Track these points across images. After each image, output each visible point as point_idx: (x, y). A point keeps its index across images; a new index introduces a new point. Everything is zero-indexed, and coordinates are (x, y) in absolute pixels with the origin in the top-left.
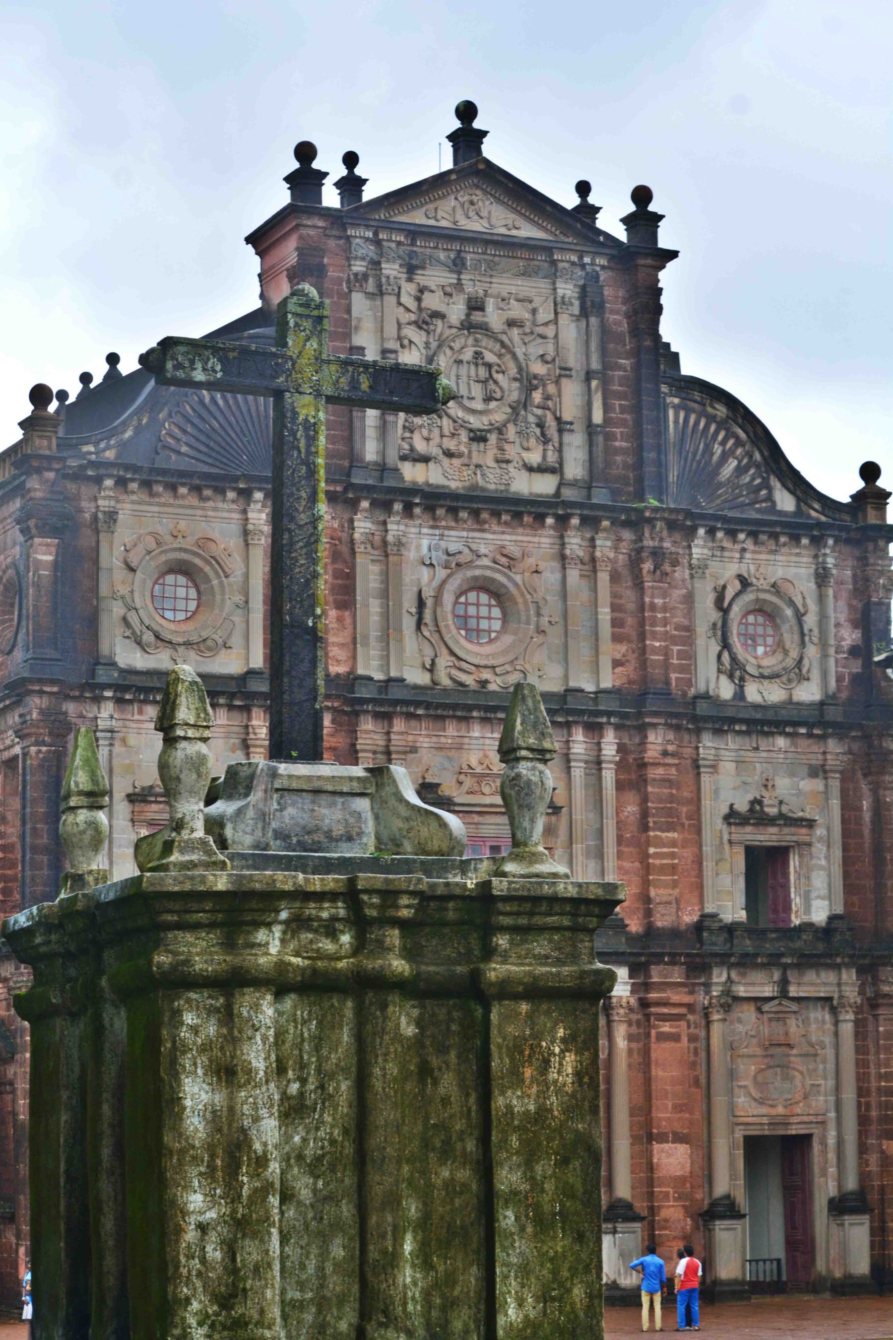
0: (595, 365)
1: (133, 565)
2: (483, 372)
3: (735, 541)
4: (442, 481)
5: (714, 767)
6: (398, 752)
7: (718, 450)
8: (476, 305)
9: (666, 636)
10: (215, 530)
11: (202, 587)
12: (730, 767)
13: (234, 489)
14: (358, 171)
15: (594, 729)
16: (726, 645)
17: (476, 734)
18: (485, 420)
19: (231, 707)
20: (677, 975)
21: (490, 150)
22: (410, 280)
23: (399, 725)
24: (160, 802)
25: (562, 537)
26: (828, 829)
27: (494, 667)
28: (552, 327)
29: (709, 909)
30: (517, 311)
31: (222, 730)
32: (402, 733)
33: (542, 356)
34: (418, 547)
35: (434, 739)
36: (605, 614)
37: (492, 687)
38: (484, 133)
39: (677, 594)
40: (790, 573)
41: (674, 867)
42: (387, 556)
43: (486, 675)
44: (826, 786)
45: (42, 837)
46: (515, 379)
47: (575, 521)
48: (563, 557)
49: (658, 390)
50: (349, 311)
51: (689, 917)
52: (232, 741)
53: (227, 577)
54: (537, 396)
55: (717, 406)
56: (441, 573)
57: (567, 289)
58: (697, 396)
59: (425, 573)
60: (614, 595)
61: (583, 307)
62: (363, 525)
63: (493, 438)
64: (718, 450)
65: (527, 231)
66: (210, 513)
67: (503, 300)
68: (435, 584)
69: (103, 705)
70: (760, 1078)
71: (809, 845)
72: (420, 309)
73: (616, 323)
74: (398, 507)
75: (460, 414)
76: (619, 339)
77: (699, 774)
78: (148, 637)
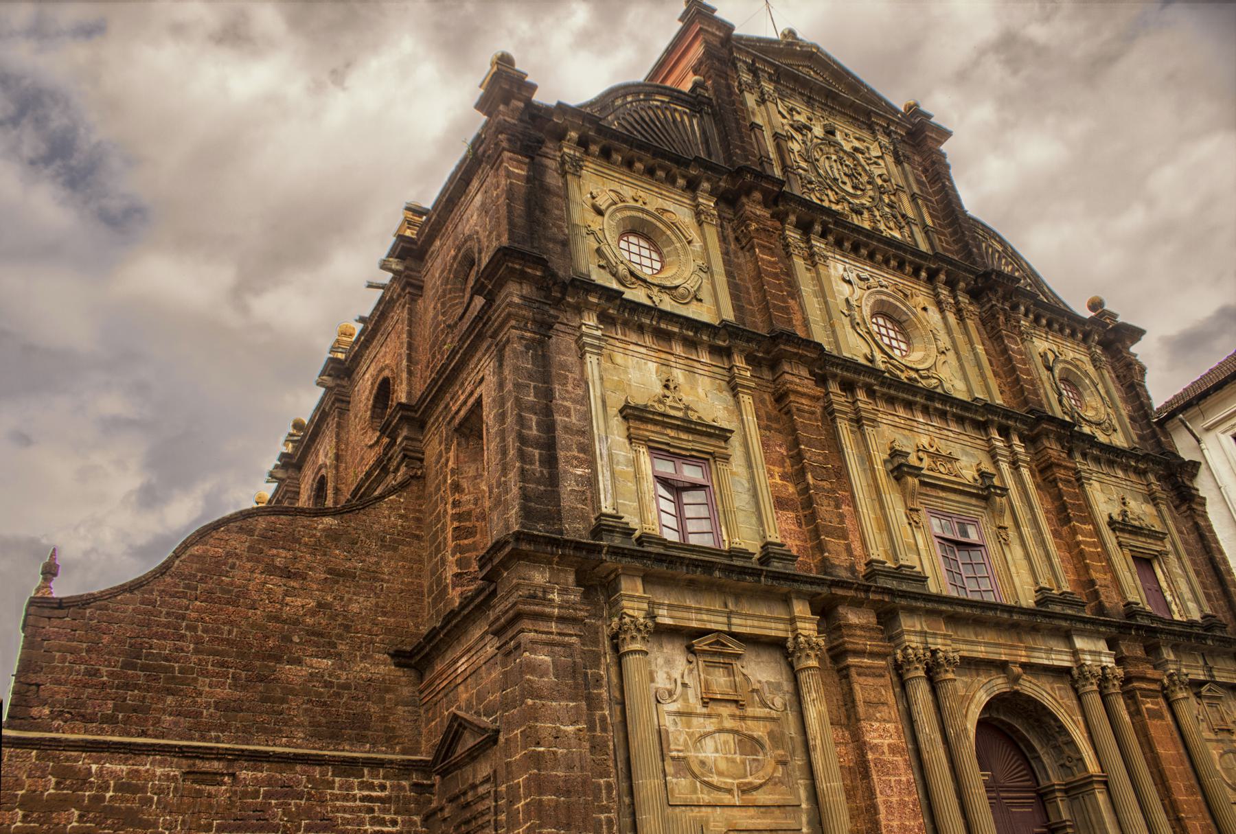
1: (603, 207)
6: (868, 419)
8: (830, 132)
10: (669, 206)
11: (665, 250)
12: (1096, 485)
13: (684, 177)
15: (1005, 432)
17: (921, 420)
19: (715, 351)
23: (861, 395)
24: (656, 423)
25: (934, 289)
26: (1174, 544)
27: (917, 371)
30: (857, 144)
31: (706, 368)
32: (865, 403)
33: (880, 176)
34: (835, 268)
35: (890, 417)
36: (980, 348)
37: (920, 385)
40: (1078, 356)
42: (814, 265)
43: (914, 375)
44: (1159, 511)
45: (530, 428)
46: (869, 183)
47: (942, 277)
48: (939, 304)
52: (718, 381)
53: (689, 242)
56: (858, 292)
57: (885, 140)
59: (846, 286)
62: (793, 235)
63: (866, 214)
66: (664, 192)
67: (846, 135)
68: (856, 296)
69: (585, 314)
71: (1167, 554)
74: (818, 228)
77: (1081, 485)
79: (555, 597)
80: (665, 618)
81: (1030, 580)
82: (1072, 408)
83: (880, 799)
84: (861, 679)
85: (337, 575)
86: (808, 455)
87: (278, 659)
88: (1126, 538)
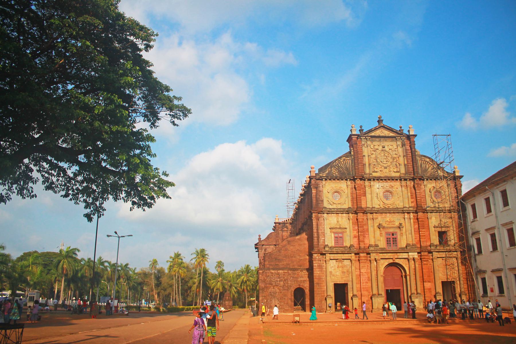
0: (405, 154)
2: (385, 157)
3: (432, 181)
4: (380, 175)
5: (431, 218)
7: (428, 166)
9: (420, 197)
14: (362, 128)
16: (432, 198)
18: (386, 165)
20: (426, 253)
21: (385, 123)
22: (372, 144)
23: (374, 214)
28: (397, 149)
29: (432, 242)
30: (390, 147)
34: (376, 186)
36: (409, 194)
38: (383, 120)
39: (422, 190)
41: (424, 236)
43: (389, 205)
44: (452, 220)
47: (403, 180)
48: (401, 186)
49: (416, 158)
50: (362, 150)
51: (428, 244)
54: (395, 160)
55: (427, 159)
56: (380, 189)
57: (399, 143)
58: (423, 158)
60: (411, 191)
61: (402, 145)
63: (388, 168)
64: (428, 166)
65: (392, 134)
70: (444, 271)
72: (374, 148)
73: (408, 148)
74: (372, 180)
75: (382, 164)
76: (408, 150)
78: (332, 203)
79: (317, 258)
80: (332, 258)
81: (406, 242)
82: (433, 201)
83: (361, 279)
84: (362, 263)
85: (300, 245)
86: (359, 230)
87: (292, 257)
88: (436, 229)
